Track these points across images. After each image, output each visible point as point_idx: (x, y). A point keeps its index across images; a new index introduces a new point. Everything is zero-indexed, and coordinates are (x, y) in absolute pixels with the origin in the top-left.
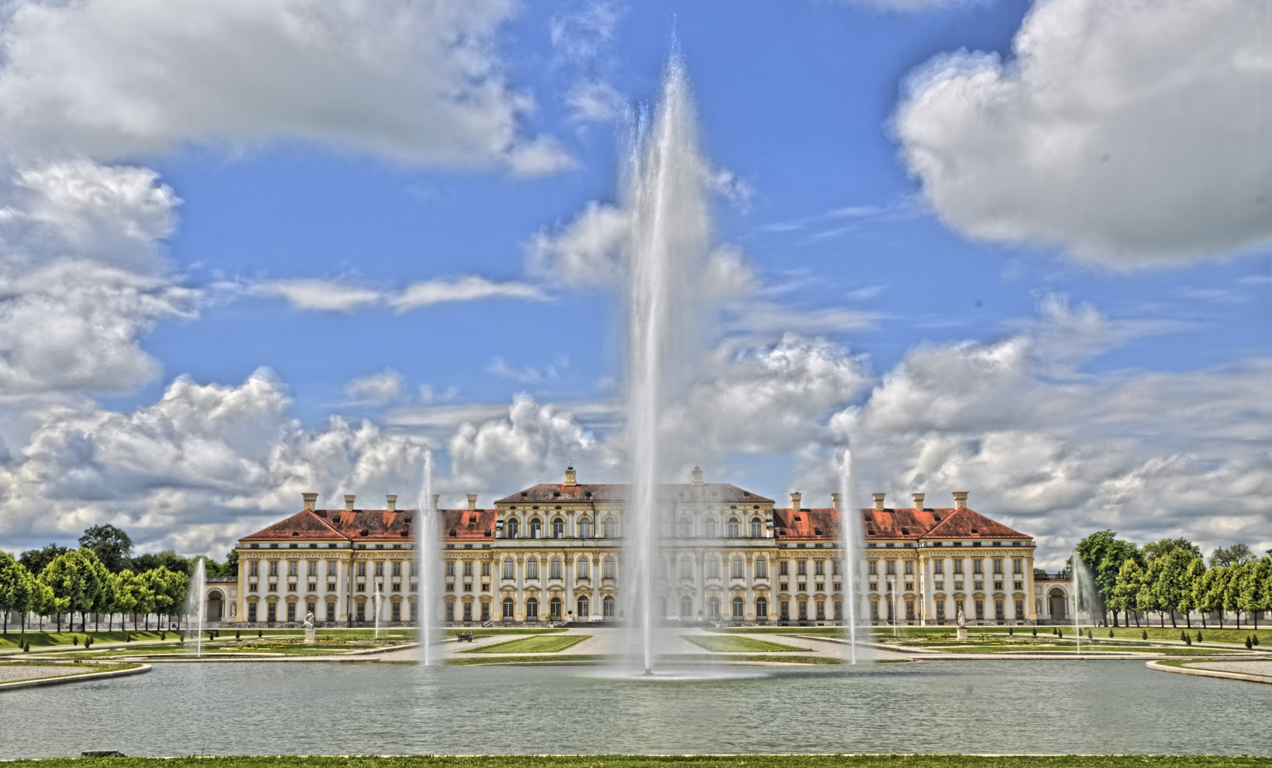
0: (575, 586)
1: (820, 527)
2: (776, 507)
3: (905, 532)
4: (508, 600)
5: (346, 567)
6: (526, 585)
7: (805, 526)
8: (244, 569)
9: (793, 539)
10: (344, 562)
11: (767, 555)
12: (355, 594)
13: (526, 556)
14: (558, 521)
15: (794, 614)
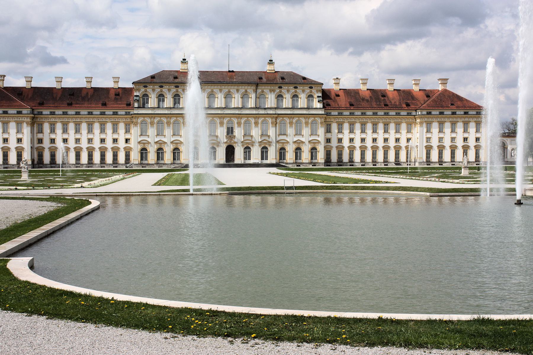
1: (353, 101)
2: (324, 87)
3: (408, 105)
6: (157, 140)
9: (335, 109)
10: (27, 123)
11: (319, 120)
13: (156, 120)
15: (334, 158)
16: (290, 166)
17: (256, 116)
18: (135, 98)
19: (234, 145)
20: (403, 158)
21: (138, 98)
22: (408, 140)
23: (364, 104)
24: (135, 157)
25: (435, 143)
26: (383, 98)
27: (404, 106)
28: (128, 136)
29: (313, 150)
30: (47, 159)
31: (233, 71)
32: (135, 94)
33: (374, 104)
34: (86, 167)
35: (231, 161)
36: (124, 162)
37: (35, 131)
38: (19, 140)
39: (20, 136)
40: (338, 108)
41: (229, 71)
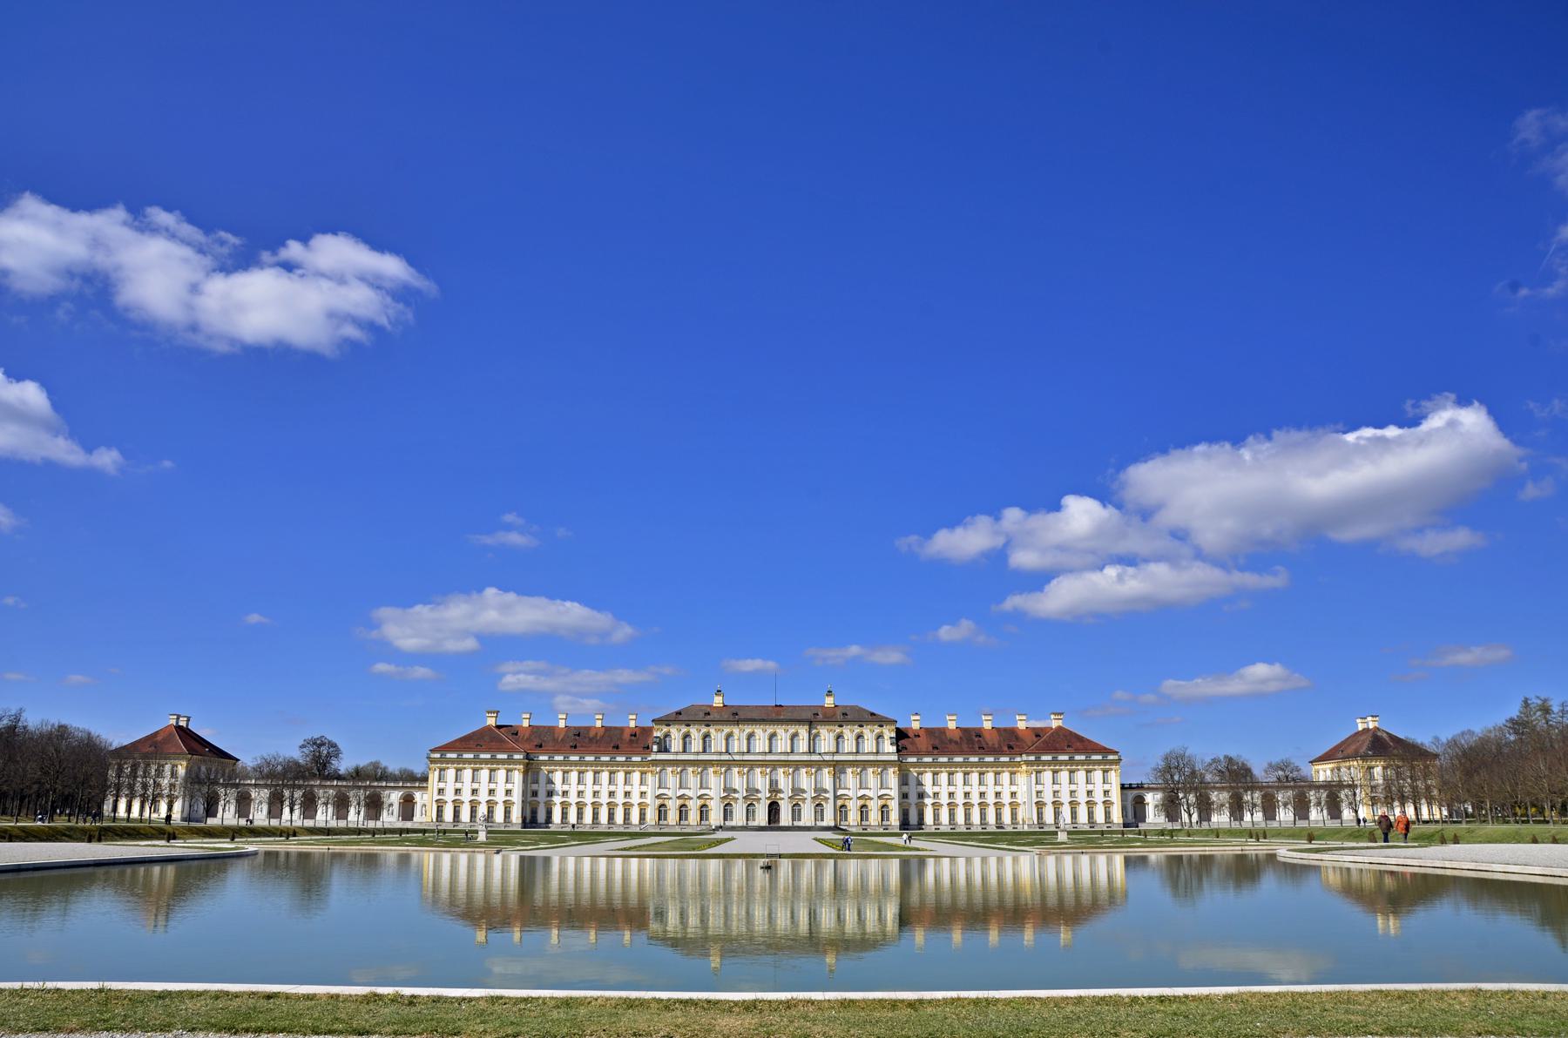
1: (937, 743)
3: (1010, 747)
7: (923, 743)
8: (434, 776)
14: (706, 736)
16: (854, 830)
17: (808, 764)
22: (1013, 794)
23: (953, 747)
24: (651, 816)
25: (1048, 798)
28: (644, 788)
29: (884, 809)
30: (541, 818)
33: (965, 747)
39: (509, 786)
40: (917, 753)
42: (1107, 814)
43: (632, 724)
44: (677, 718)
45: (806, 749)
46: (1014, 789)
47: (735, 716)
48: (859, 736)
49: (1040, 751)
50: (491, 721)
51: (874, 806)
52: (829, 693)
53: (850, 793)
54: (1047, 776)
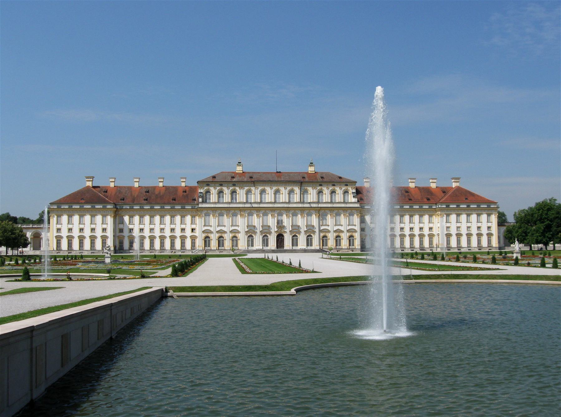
0: (246, 230)
3: (428, 199)
4: (207, 237)
5: (112, 219)
8: (54, 220)
12: (118, 234)
18: (199, 194)
19: (284, 235)
20: (426, 244)
21: (202, 195)
22: (431, 229)
25: (453, 231)
26: (407, 194)
27: (425, 200)
28: (194, 226)
29: (351, 239)
30: (126, 246)
31: (280, 172)
32: (199, 191)
34: (159, 252)
35: (281, 247)
36: (190, 249)
37: (117, 223)
38: (104, 230)
39: (104, 226)
41: (277, 172)
42: (489, 241)
43: (183, 185)
44: (213, 181)
45: (298, 200)
46: (431, 225)
47: (253, 180)
48: (333, 192)
49: (420, 202)
50: (89, 184)
51: (345, 237)
52: (311, 164)
53: (329, 228)
54: (453, 217)
